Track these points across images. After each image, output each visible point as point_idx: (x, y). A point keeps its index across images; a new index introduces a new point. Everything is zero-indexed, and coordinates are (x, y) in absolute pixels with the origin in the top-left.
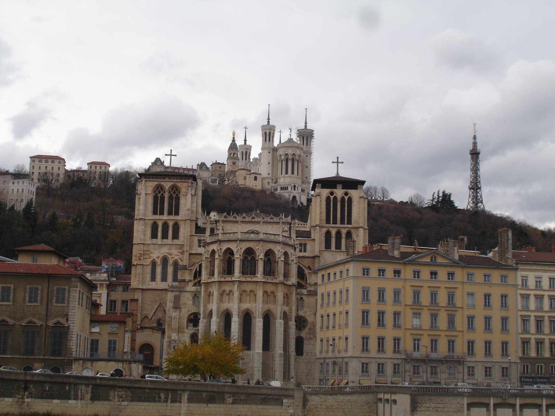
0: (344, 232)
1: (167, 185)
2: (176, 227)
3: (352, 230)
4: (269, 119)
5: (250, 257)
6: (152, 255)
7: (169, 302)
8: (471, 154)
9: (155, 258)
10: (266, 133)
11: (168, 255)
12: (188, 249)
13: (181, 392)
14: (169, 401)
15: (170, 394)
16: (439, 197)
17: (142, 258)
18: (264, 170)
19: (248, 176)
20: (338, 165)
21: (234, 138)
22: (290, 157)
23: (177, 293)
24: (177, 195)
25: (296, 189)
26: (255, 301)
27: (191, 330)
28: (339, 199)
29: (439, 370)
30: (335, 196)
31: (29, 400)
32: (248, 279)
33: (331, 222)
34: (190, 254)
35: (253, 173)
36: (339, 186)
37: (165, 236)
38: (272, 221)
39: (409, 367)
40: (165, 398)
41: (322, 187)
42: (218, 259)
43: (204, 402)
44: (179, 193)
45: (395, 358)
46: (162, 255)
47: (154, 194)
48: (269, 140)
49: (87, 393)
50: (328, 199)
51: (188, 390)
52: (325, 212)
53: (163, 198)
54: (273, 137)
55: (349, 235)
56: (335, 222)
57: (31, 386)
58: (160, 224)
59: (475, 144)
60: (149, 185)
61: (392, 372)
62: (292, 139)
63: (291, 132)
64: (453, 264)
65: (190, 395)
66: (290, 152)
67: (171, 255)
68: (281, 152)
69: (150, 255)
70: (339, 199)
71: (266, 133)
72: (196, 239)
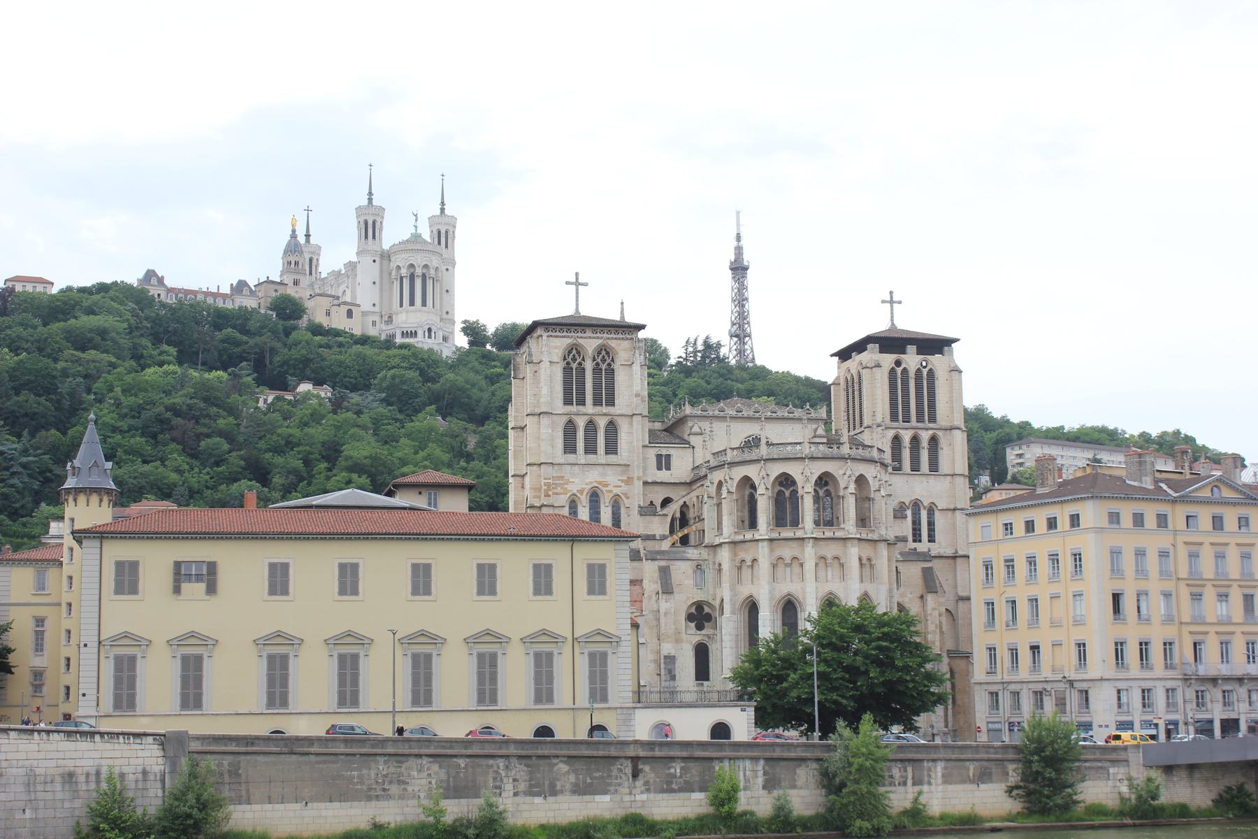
0: (925, 436)
1: (590, 344)
2: (612, 428)
3: (940, 433)
4: (370, 193)
5: (789, 491)
6: (569, 487)
7: (650, 581)
8: (731, 269)
9: (575, 491)
10: (366, 223)
11: (600, 487)
12: (641, 474)
13: (930, 764)
14: (910, 782)
15: (910, 769)
16: (695, 352)
17: (550, 493)
18: (366, 295)
19: (334, 309)
20: (577, 290)
21: (294, 231)
22: (419, 271)
23: (663, 563)
24: (609, 365)
25: (433, 334)
26: (843, 578)
27: (694, 637)
28: (912, 374)
29: (1234, 697)
30: (905, 369)
31: (644, 797)
32: (829, 534)
33: (900, 418)
34: (645, 483)
35: (345, 303)
36: (911, 349)
37: (591, 449)
38: (791, 415)
39: (1190, 694)
40: (901, 776)
41: (883, 350)
42: (765, 497)
43: (972, 782)
44: (613, 360)
45: (1168, 679)
46: (590, 487)
47: (563, 364)
48: (374, 237)
49: (757, 777)
50: (892, 371)
51: (941, 760)
52: (888, 399)
53: (582, 371)
54: (381, 230)
55: (934, 441)
56: (907, 419)
57: (647, 768)
58: (581, 423)
59: (739, 251)
60: (553, 344)
61: (1165, 705)
62: (420, 236)
63: (416, 220)
64: (1247, 501)
65: (945, 768)
66: (419, 260)
67: (606, 485)
68: (400, 260)
69: (565, 486)
70: (912, 374)
71: (366, 223)
72: (652, 454)
